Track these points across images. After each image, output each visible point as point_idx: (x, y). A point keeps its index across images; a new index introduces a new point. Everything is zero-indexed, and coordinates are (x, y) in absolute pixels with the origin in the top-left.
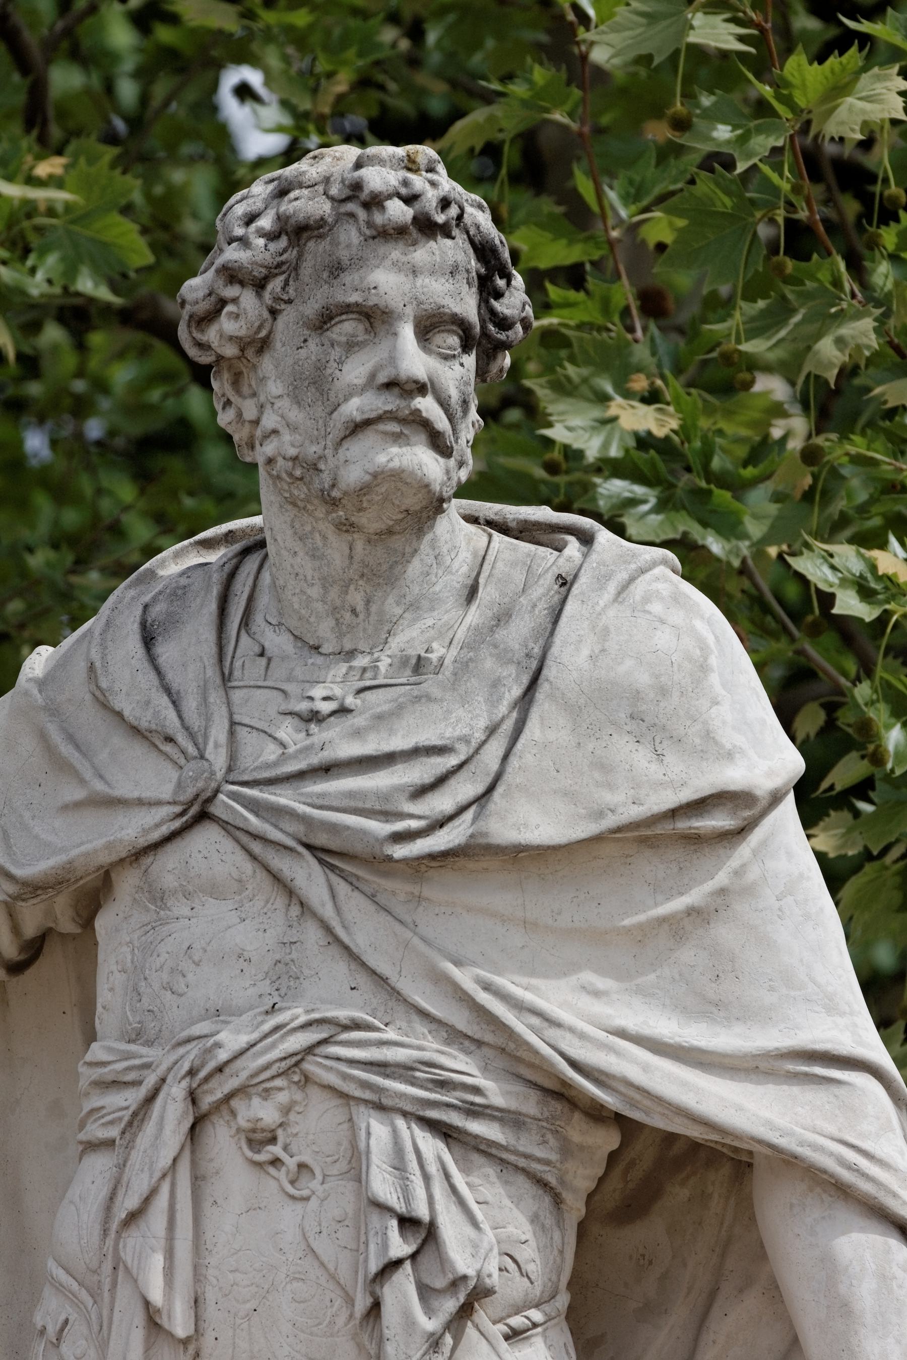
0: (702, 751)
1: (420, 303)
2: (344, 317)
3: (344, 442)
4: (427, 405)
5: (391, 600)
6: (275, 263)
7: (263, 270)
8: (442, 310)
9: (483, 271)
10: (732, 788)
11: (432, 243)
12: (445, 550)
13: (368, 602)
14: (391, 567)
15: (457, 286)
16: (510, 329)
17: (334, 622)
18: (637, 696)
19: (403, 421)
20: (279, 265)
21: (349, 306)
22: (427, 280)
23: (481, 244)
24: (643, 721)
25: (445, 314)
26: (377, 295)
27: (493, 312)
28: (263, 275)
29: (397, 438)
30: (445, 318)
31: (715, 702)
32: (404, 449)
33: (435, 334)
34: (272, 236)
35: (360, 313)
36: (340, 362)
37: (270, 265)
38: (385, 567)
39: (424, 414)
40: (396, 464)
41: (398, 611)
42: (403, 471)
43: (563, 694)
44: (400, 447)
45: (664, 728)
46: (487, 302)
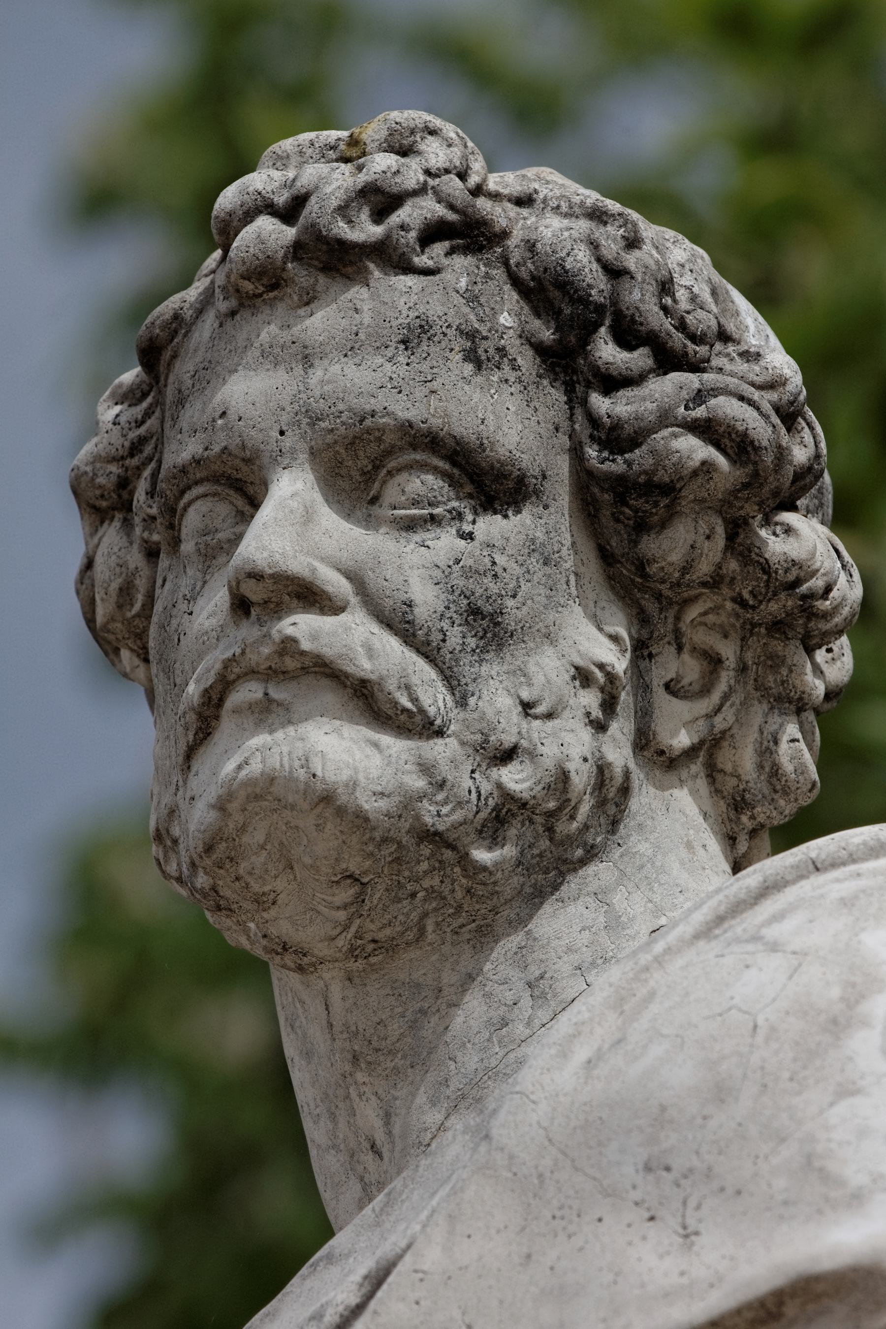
0: (786, 1203)
1: (315, 419)
2: (187, 497)
3: (196, 765)
4: (353, 638)
5: (421, 1099)
6: (127, 444)
7: (114, 468)
8: (368, 422)
9: (547, 335)
10: (827, 1264)
11: (358, 293)
12: (565, 966)
13: (388, 1117)
14: (414, 1025)
15: (425, 367)
16: (638, 445)
17: (358, 1187)
18: (662, 1117)
19: (272, 674)
20: (135, 448)
21: (184, 470)
22: (336, 368)
23: (533, 278)
24: (668, 1169)
25: (382, 430)
26: (227, 428)
27: (593, 421)
28: (114, 478)
29: (266, 713)
30: (389, 438)
31: (847, 1090)
32: (280, 735)
33: (384, 482)
34: (138, 394)
35: (215, 478)
36: (191, 599)
37: (121, 453)
38: (395, 1028)
39: (305, 645)
40: (256, 767)
41: (434, 1117)
42: (272, 780)
43: (511, 1157)
44: (271, 732)
45: (709, 1173)
46: (584, 402)
